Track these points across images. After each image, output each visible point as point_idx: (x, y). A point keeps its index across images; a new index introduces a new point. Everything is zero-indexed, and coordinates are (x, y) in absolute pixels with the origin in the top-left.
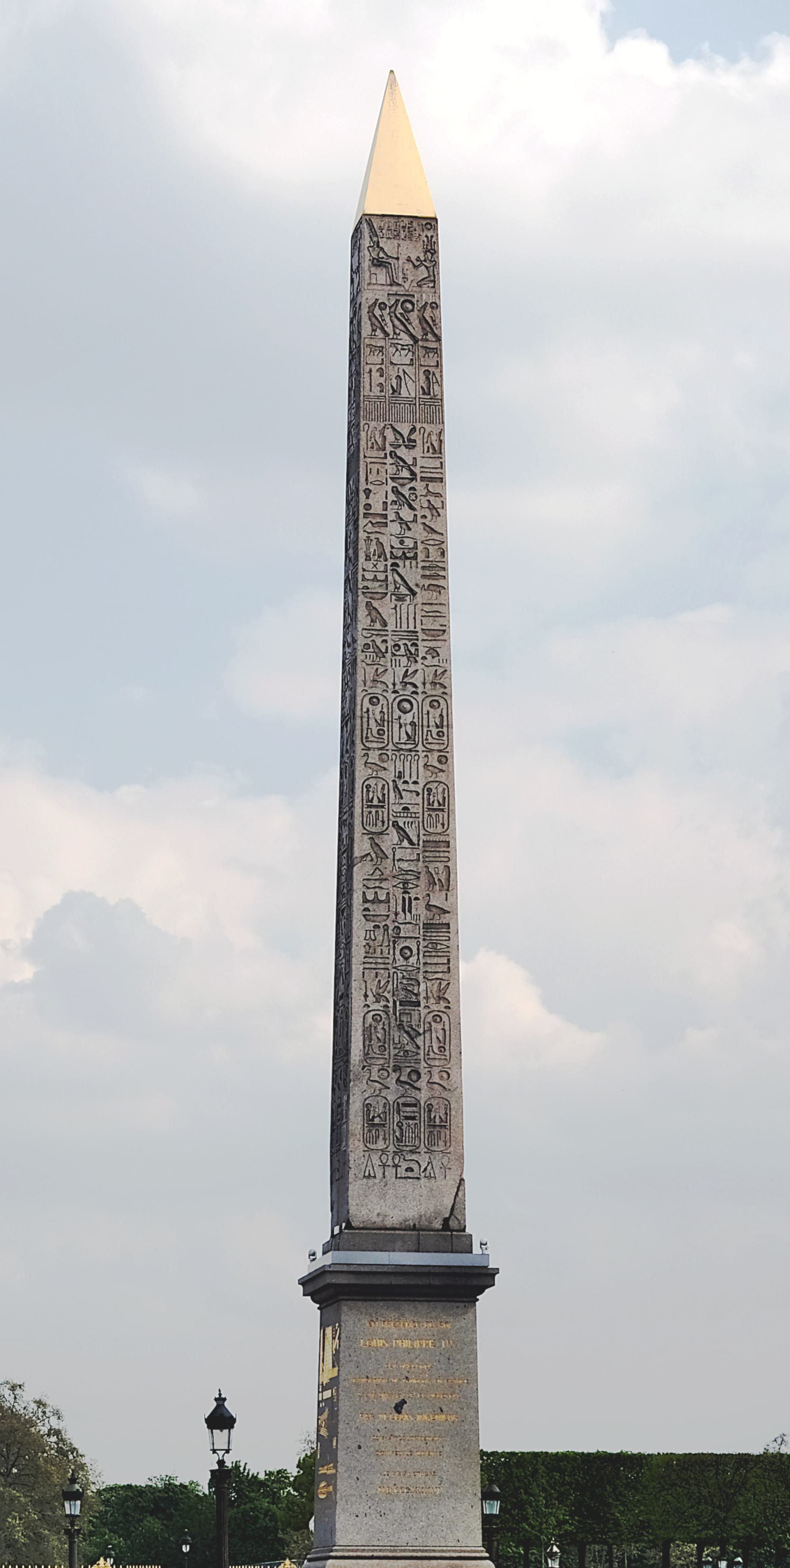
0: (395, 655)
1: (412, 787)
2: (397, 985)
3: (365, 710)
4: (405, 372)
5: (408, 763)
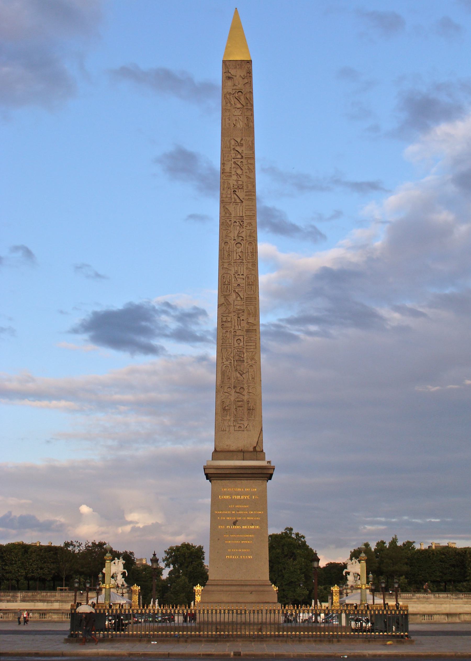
0: (234, 226)
1: (241, 276)
3: (222, 247)
5: (240, 267)
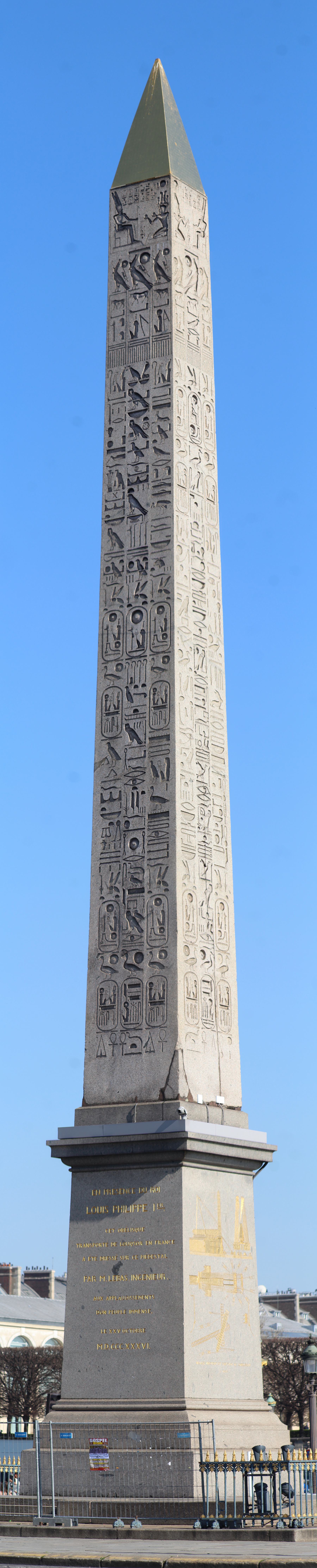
1: (141, 690)
4: (141, 317)
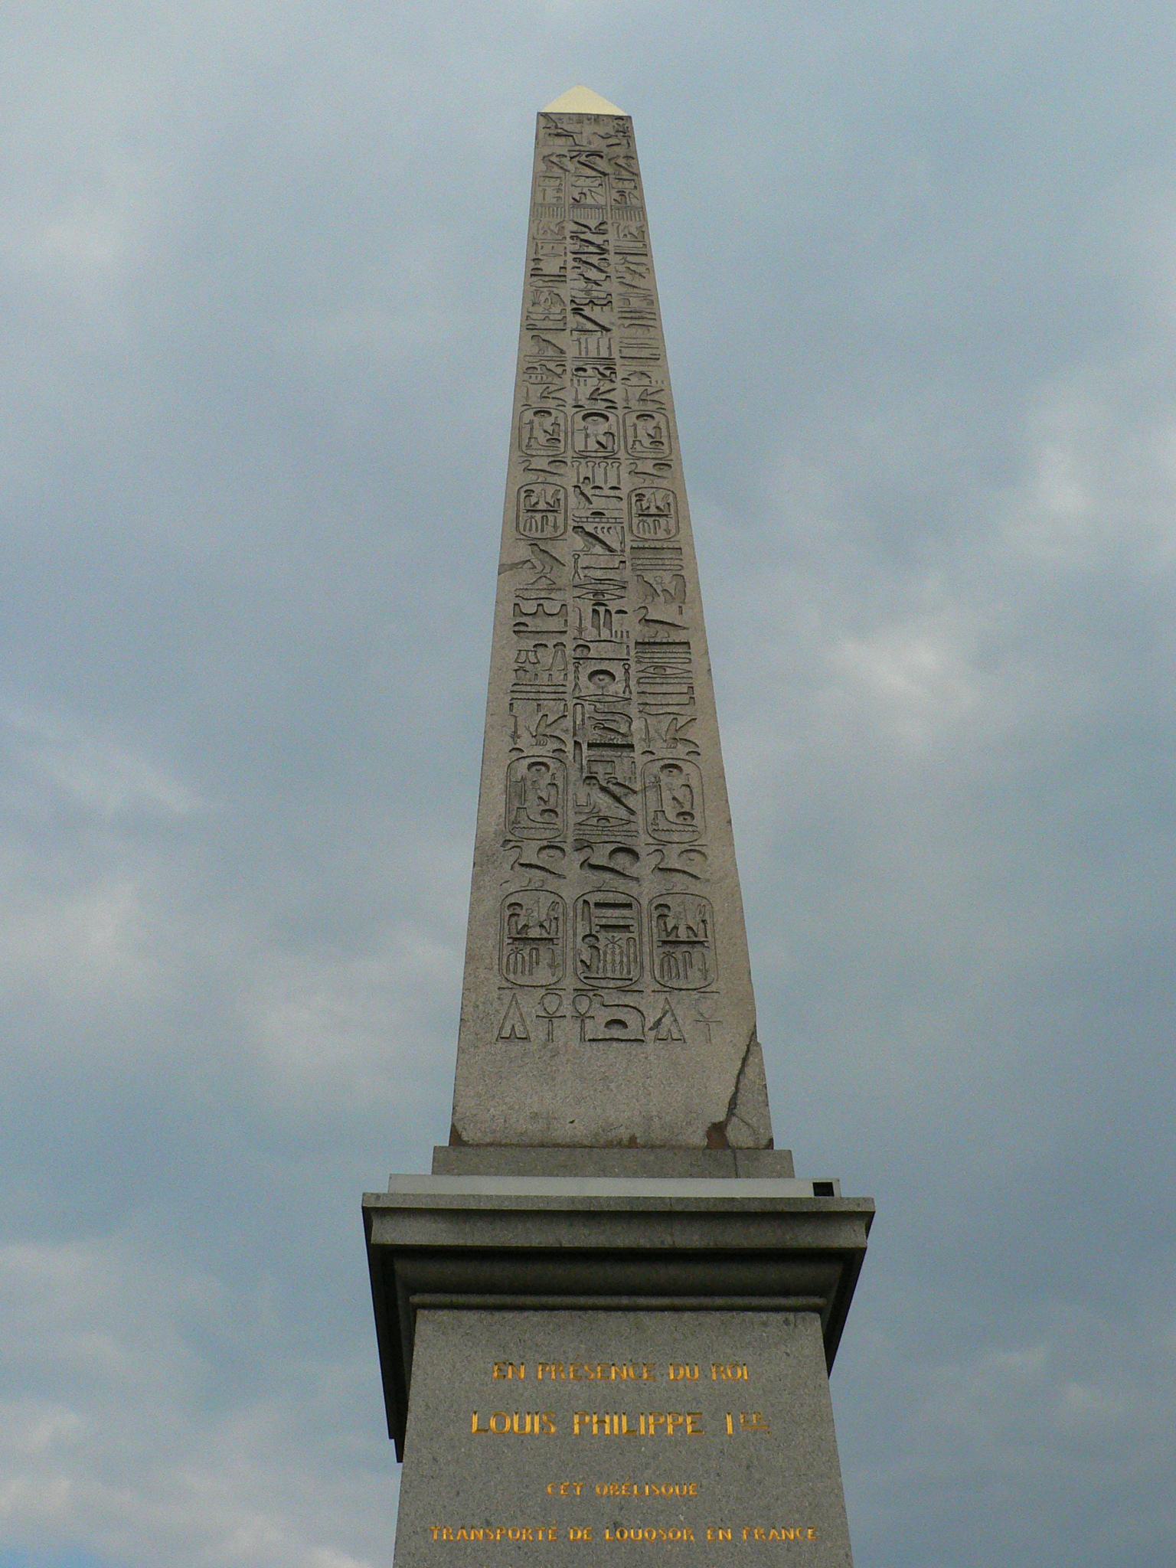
2: (583, 720)
